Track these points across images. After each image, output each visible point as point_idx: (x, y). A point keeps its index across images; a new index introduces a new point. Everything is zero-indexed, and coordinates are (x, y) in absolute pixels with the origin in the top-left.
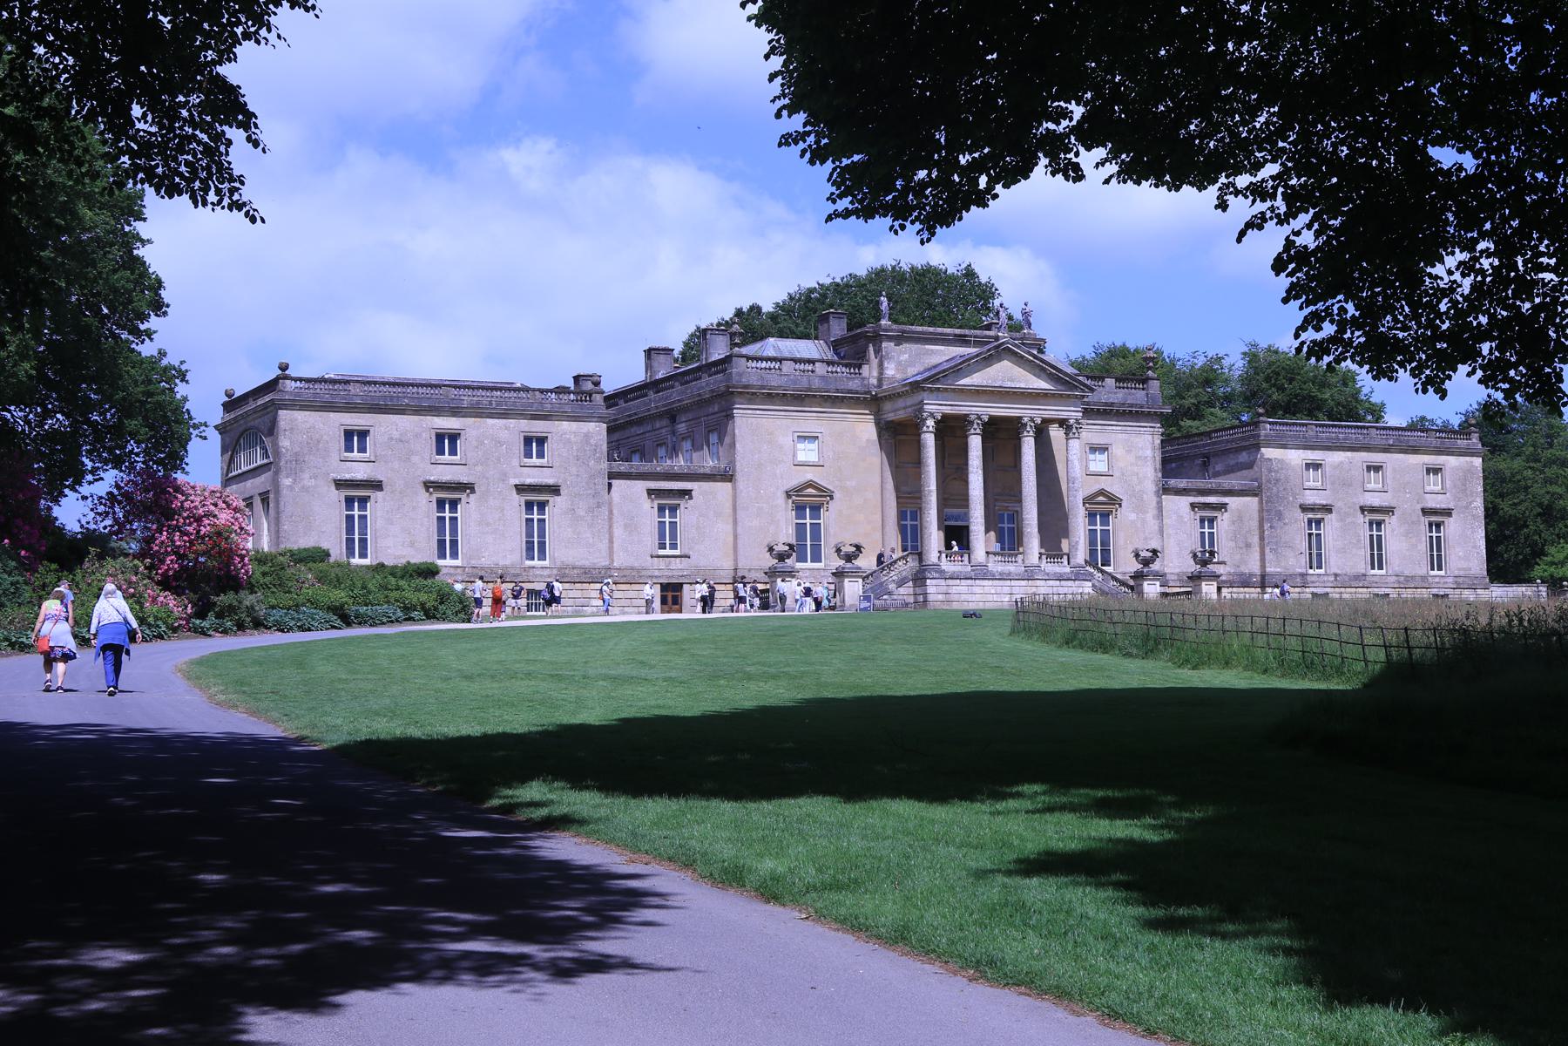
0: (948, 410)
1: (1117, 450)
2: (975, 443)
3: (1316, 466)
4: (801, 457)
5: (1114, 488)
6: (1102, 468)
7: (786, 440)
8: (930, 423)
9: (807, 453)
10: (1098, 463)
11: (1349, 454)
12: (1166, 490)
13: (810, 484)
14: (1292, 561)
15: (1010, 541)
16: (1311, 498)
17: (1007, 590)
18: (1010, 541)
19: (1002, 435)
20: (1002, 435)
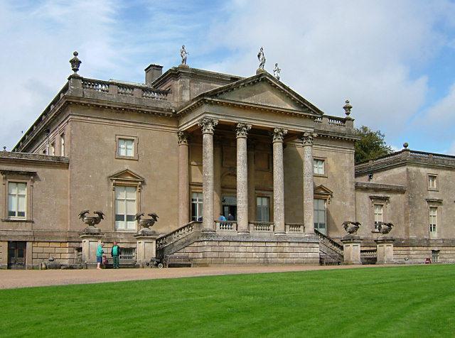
0: (223, 119)
1: (330, 161)
2: (242, 144)
3: (433, 177)
4: (123, 153)
5: (328, 186)
6: (321, 172)
7: (111, 141)
8: (210, 127)
9: (128, 150)
10: (320, 169)
11: (449, 172)
12: (358, 188)
13: (126, 173)
14: (423, 232)
15: (261, 217)
16: (432, 196)
17: (262, 249)
18: (261, 217)
19: (260, 141)
20: (260, 141)
